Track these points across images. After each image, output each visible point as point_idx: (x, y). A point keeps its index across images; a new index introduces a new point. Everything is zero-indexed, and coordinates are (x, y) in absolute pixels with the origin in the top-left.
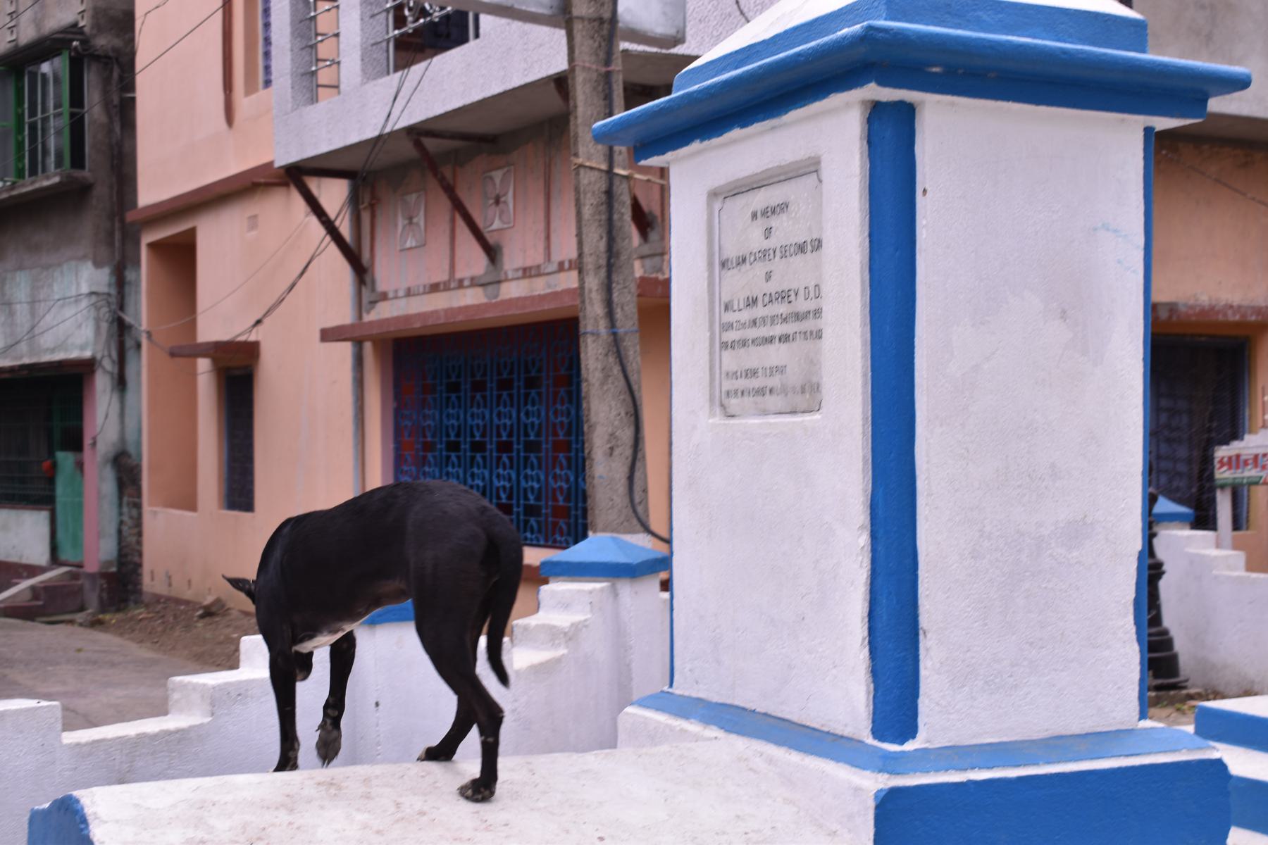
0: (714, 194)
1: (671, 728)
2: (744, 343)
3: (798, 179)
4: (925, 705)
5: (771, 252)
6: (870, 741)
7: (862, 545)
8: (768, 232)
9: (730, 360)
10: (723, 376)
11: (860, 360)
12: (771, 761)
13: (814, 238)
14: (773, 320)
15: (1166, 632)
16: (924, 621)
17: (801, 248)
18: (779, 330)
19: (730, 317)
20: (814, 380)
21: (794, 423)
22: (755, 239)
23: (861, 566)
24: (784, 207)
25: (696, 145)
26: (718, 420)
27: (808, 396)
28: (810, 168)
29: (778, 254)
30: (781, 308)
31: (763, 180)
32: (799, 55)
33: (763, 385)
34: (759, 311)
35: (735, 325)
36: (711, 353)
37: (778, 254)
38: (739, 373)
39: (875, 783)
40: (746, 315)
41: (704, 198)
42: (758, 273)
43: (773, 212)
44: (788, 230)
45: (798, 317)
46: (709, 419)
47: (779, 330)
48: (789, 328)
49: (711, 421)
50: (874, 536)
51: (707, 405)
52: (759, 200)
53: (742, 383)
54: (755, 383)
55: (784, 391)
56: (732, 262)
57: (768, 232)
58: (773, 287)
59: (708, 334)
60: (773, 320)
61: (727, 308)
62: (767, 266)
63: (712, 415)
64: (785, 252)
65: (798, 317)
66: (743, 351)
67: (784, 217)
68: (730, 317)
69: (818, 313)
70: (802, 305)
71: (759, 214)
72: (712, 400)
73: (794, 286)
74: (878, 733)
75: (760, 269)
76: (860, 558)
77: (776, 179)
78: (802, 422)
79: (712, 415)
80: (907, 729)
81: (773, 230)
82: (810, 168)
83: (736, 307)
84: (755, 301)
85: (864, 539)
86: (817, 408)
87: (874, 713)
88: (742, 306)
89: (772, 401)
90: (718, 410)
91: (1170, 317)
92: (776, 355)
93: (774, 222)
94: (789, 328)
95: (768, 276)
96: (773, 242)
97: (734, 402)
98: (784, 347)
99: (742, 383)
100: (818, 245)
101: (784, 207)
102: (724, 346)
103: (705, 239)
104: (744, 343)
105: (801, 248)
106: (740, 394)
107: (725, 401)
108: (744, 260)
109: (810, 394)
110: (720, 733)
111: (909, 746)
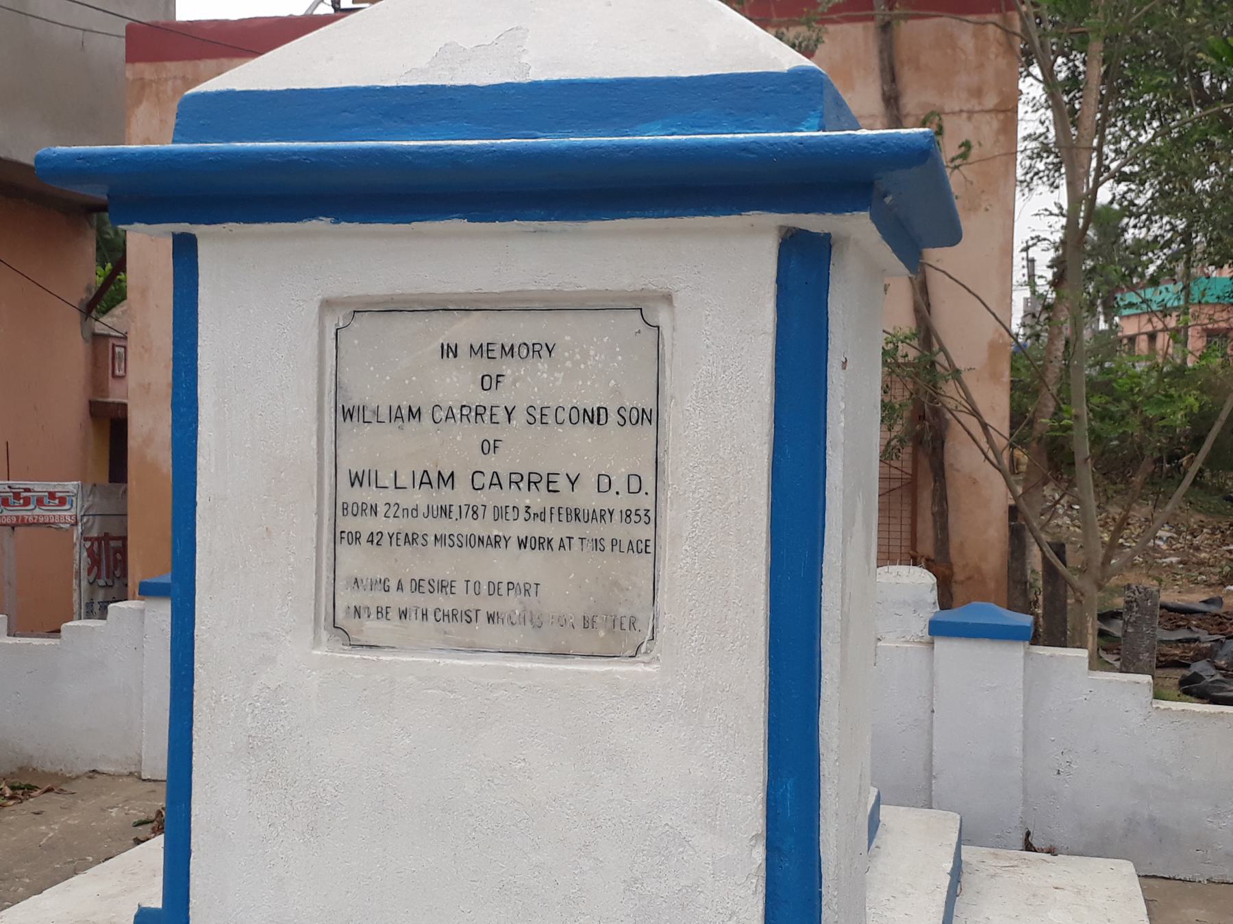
0: (327, 305)
2: (411, 539)
3: (588, 319)
5: (501, 415)
7: (760, 862)
8: (491, 382)
9: (353, 560)
10: (340, 584)
11: (763, 596)
13: (628, 405)
14: (500, 513)
17: (594, 417)
18: (518, 528)
20: (622, 611)
21: (580, 672)
23: (755, 893)
24: (540, 350)
25: (321, 225)
27: (602, 634)
29: (520, 417)
30: (537, 499)
31: (476, 301)
33: (473, 607)
34: (460, 495)
35: (381, 509)
36: (318, 548)
37: (520, 417)
38: (393, 584)
40: (420, 497)
41: (315, 307)
42: (459, 438)
46: (313, 649)
47: (518, 528)
48: (553, 530)
49: (315, 652)
51: (310, 627)
52: (465, 331)
54: (446, 603)
55: (535, 621)
56: (376, 412)
57: (491, 382)
58: (501, 463)
59: (315, 519)
60: (500, 513)
61: (356, 480)
63: (317, 643)
64: (538, 416)
67: (542, 365)
68: (365, 495)
69: (651, 517)
70: (587, 498)
71: (463, 350)
72: (316, 620)
75: (467, 436)
76: (754, 881)
77: (507, 307)
78: (604, 674)
79: (317, 643)
81: (505, 381)
83: (386, 480)
84: (449, 480)
86: (630, 652)
88: (404, 480)
89: (483, 631)
90: (324, 635)
93: (508, 368)
94: (553, 530)
97: (372, 628)
98: (529, 556)
101: (536, 350)
102: (355, 538)
103: (314, 373)
104: (411, 539)
105: (594, 417)
106: (393, 614)
107: (351, 624)
108: (415, 414)
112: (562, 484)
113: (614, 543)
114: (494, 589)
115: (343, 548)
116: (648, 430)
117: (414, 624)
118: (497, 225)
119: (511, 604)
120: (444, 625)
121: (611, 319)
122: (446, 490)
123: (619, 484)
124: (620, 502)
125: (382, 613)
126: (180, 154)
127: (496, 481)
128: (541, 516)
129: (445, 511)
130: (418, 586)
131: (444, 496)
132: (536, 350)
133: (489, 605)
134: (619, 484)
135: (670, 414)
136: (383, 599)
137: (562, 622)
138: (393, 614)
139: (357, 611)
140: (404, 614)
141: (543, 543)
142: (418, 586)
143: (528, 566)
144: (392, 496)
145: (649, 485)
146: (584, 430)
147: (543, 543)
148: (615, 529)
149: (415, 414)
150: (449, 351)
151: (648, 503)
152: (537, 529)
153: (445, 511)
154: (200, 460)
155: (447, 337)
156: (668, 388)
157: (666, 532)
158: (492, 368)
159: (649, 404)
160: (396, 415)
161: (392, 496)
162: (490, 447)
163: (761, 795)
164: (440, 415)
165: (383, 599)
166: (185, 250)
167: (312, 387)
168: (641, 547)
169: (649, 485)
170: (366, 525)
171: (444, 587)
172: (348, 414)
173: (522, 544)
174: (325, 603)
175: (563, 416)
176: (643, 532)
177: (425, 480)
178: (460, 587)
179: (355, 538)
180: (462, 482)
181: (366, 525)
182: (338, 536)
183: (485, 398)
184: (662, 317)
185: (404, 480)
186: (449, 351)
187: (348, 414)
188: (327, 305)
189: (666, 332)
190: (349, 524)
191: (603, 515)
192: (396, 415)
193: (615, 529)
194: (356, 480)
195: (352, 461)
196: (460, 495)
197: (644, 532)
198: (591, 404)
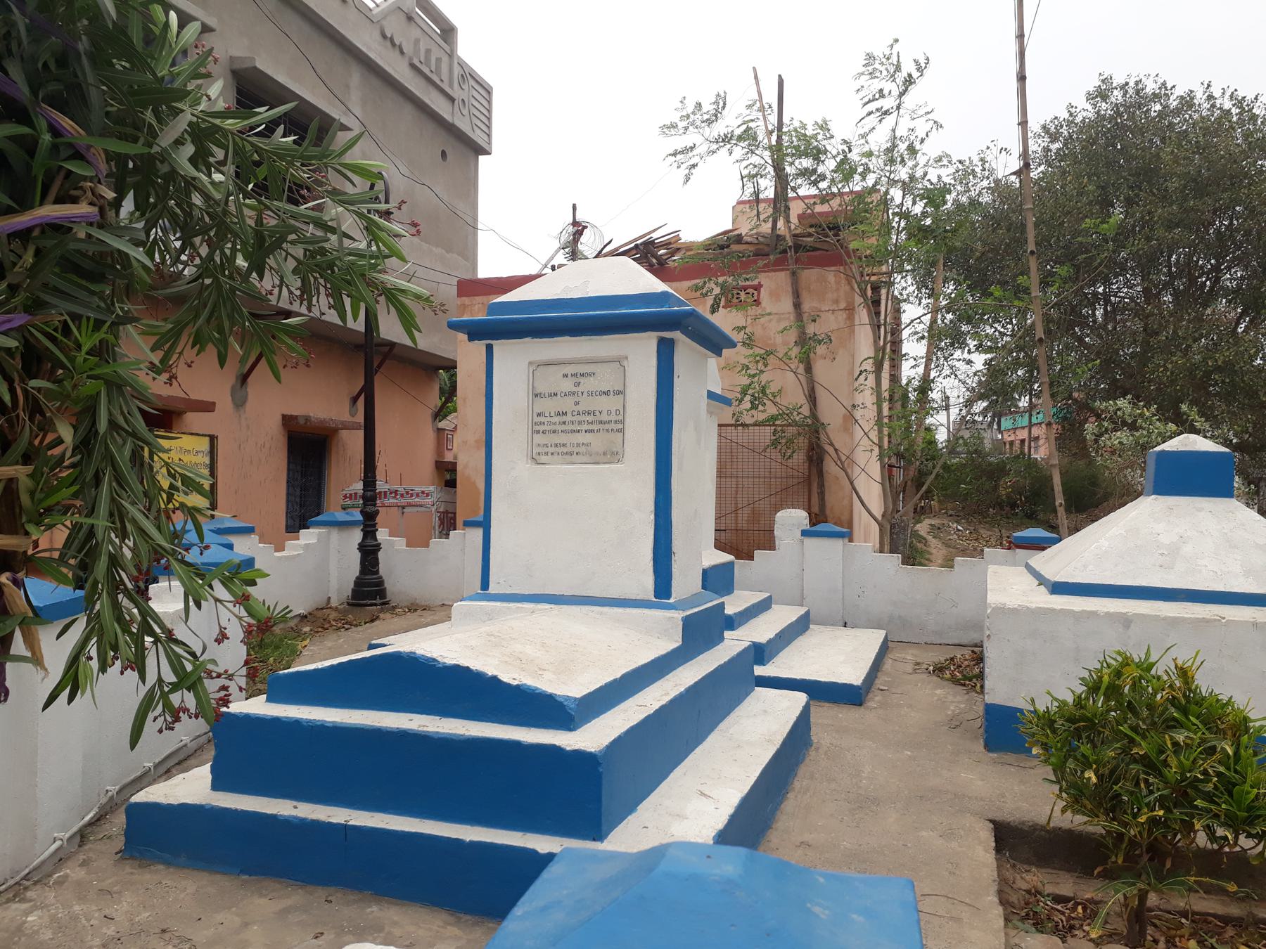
0: (530, 363)
1: (508, 608)
3: (605, 364)
4: (674, 583)
5: (580, 393)
6: (655, 600)
8: (577, 384)
9: (538, 439)
12: (601, 613)
14: (580, 423)
15: (381, 577)
16: (674, 549)
17: (606, 393)
18: (585, 427)
19: (537, 419)
22: (567, 385)
26: (530, 465)
28: (619, 361)
29: (586, 394)
30: (590, 418)
32: (643, 313)
34: (569, 418)
37: (586, 394)
39: (678, 615)
40: (557, 419)
43: (582, 375)
44: (587, 384)
45: (601, 422)
48: (595, 427)
50: (656, 515)
52: (570, 370)
53: (550, 450)
57: (577, 384)
58: (580, 408)
60: (580, 423)
61: (539, 415)
62: (576, 399)
63: (527, 463)
64: (591, 394)
65: (601, 422)
66: (553, 435)
69: (622, 422)
70: (604, 417)
71: (569, 376)
73: (598, 408)
74: (656, 597)
75: (571, 400)
80: (669, 596)
81: (581, 384)
82: (619, 361)
83: (547, 415)
85: (652, 517)
87: (655, 588)
88: (552, 414)
90: (529, 461)
91: (306, 423)
92: (580, 438)
93: (582, 380)
94: (595, 427)
95: (577, 403)
96: (580, 389)
97: (543, 459)
99: (550, 450)
100: (621, 392)
101: (589, 375)
102: (538, 432)
105: (606, 393)
106: (550, 454)
108: (555, 395)
109: (611, 456)
110: (552, 606)
111: (672, 601)
112: (597, 413)
113: (612, 430)
114: (578, 445)
115: (535, 435)
116: (621, 396)
117: (555, 457)
118: (578, 338)
119: (582, 449)
120: (564, 456)
121: (612, 364)
122: (564, 417)
123: (614, 413)
124: (613, 418)
125: (546, 454)
126: (488, 319)
127: (579, 413)
128: (591, 423)
129: (564, 423)
130: (556, 445)
131: (564, 418)
132: (589, 375)
133: (577, 450)
134: (614, 413)
135: (628, 392)
136: (546, 450)
137: (597, 453)
138: (550, 454)
139: (539, 454)
140: (552, 454)
141: (592, 431)
142: (556, 445)
143: (588, 438)
144: (549, 419)
145: (622, 413)
146: (604, 397)
147: (592, 431)
148: (612, 426)
149: (555, 395)
150: (565, 376)
151: (620, 417)
152: (590, 427)
153: (564, 423)
154: (494, 410)
155: (565, 371)
156: (627, 384)
157: (626, 426)
158: (578, 380)
159: (622, 389)
160: (550, 395)
161: (549, 419)
162: (577, 403)
163: (653, 499)
164: (563, 395)
165: (546, 450)
166: (489, 349)
167: (526, 386)
168: (619, 431)
169: (622, 413)
170: (541, 428)
171: (564, 445)
172: (536, 395)
173: (586, 431)
174: (530, 453)
175: (597, 393)
176: (620, 426)
177: (559, 414)
178: (568, 445)
179: (538, 432)
180: (569, 415)
181: (541, 428)
182: (534, 432)
183: (576, 389)
184: (625, 363)
185: (552, 414)
186: (565, 376)
187: (536, 395)
188: (530, 363)
189: (626, 368)
190: (537, 428)
191: (609, 422)
192: (550, 395)
193: (612, 426)
194: (539, 415)
195: (537, 410)
196: (569, 418)
197: (620, 426)
198: (606, 390)
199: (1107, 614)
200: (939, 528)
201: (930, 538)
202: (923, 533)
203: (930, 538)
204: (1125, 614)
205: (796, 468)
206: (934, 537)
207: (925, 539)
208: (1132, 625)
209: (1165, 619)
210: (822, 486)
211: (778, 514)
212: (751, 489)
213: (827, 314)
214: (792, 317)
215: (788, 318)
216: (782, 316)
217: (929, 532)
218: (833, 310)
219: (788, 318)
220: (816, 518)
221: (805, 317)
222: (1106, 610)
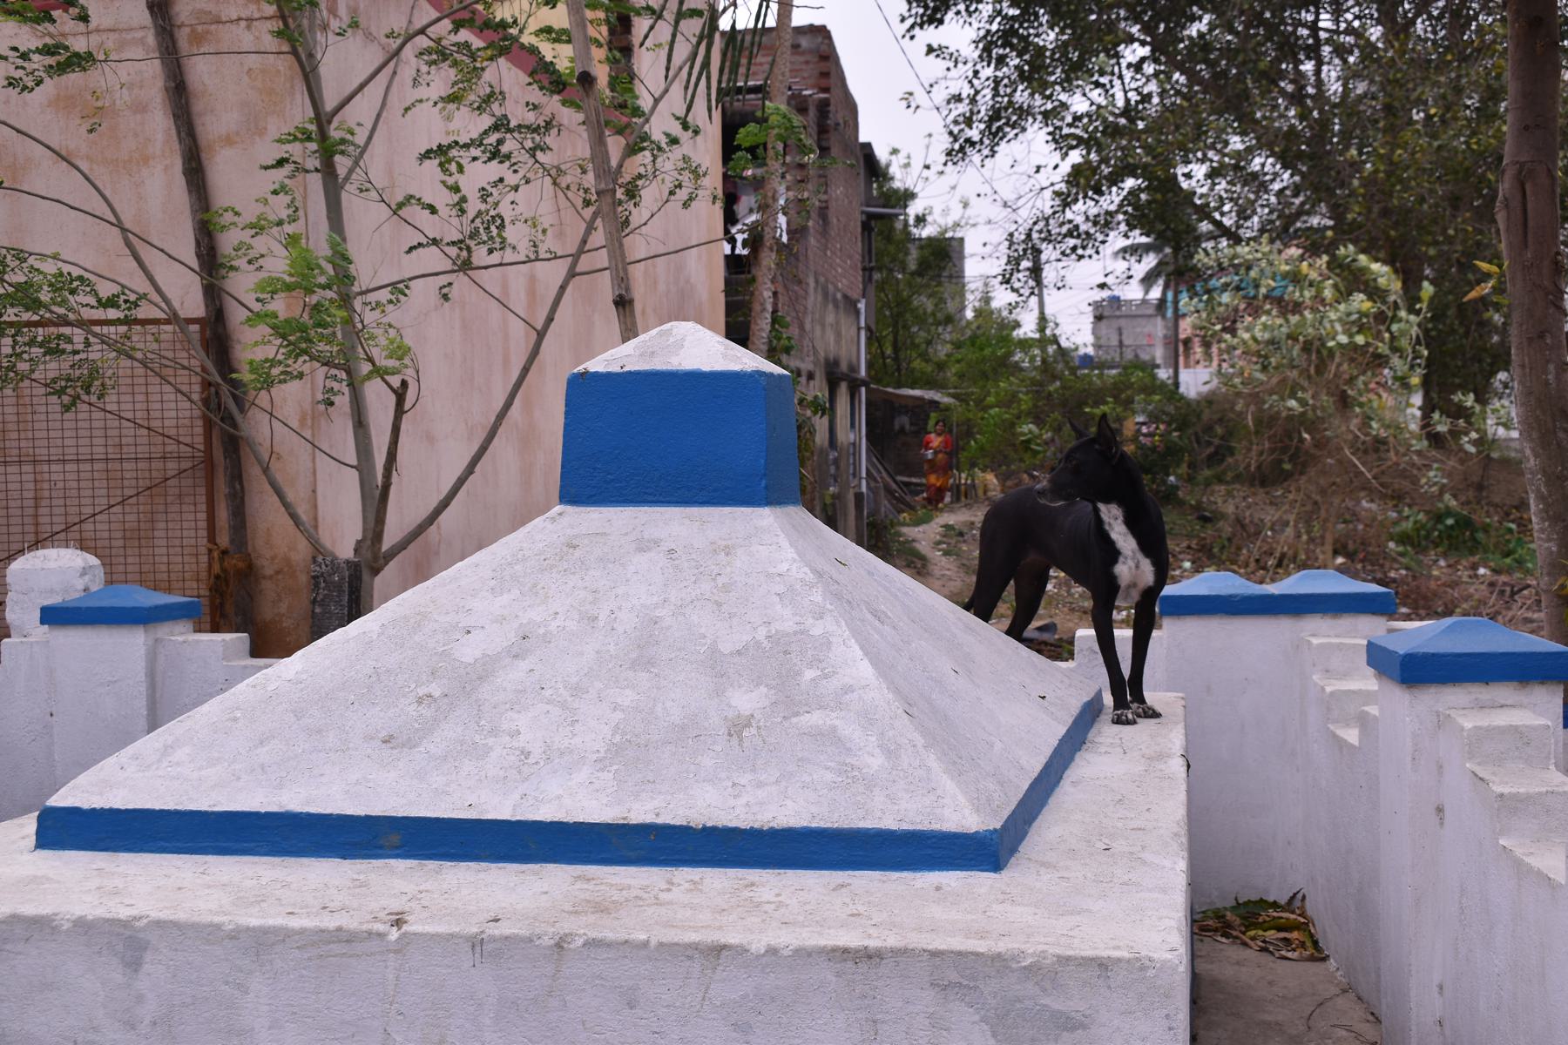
199: (84, 927)
200: (961, 534)
201: (936, 556)
202: (923, 547)
203: (936, 556)
204: (125, 924)
205: (173, 432)
206: (946, 553)
207: (923, 558)
208: (148, 956)
209: (237, 934)
210: (237, 475)
211: (16, 566)
212: (74, 493)
213: (233, 27)
214: (151, 39)
215: (142, 41)
216: (129, 36)
217: (939, 543)
218: (250, 20)
219: (142, 41)
220: (221, 560)
221: (183, 36)
222: (79, 911)
